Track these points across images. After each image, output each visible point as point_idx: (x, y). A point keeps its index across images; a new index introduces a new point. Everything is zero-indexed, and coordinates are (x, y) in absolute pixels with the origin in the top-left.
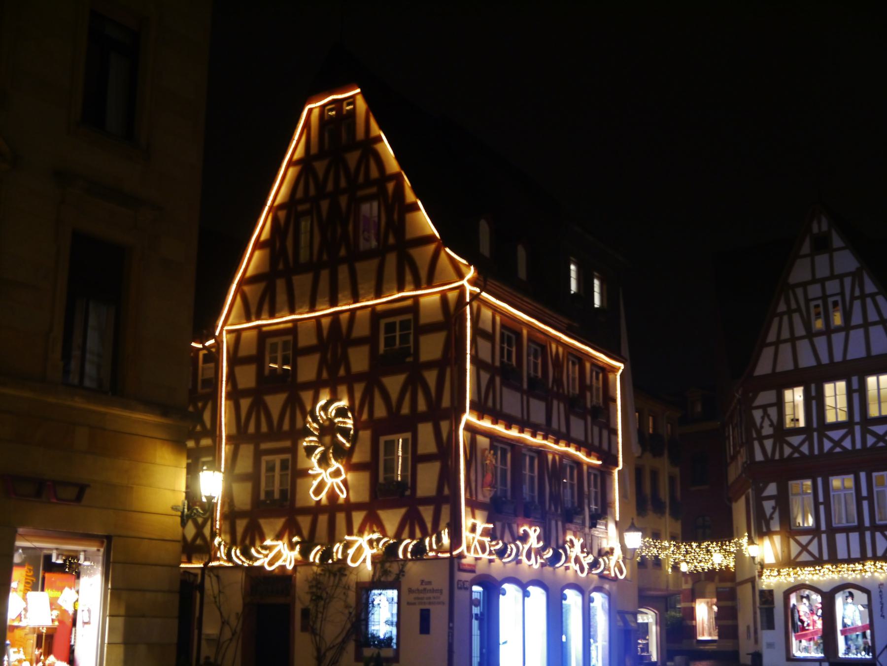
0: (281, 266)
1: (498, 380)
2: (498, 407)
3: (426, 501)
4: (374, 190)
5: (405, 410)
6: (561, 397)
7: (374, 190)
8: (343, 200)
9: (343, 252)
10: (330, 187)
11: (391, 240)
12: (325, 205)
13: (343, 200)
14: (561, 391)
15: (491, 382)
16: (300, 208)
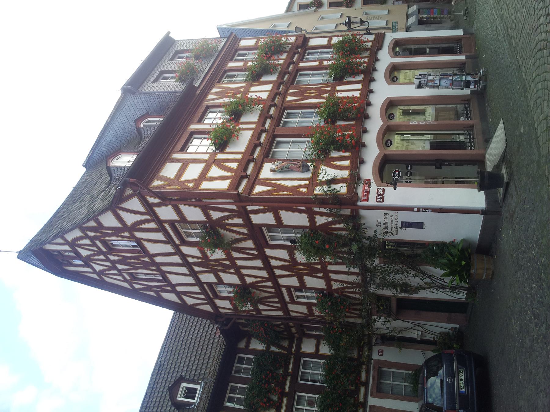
0: (169, 288)
1: (220, 156)
2: (239, 156)
3: (312, 220)
4: (98, 242)
5: (244, 230)
6: (247, 91)
7: (98, 242)
8: (112, 258)
9: (146, 259)
10: (108, 264)
11: (126, 234)
12: (120, 267)
13: (112, 258)
14: (242, 90)
15: (220, 164)
16: (128, 278)
